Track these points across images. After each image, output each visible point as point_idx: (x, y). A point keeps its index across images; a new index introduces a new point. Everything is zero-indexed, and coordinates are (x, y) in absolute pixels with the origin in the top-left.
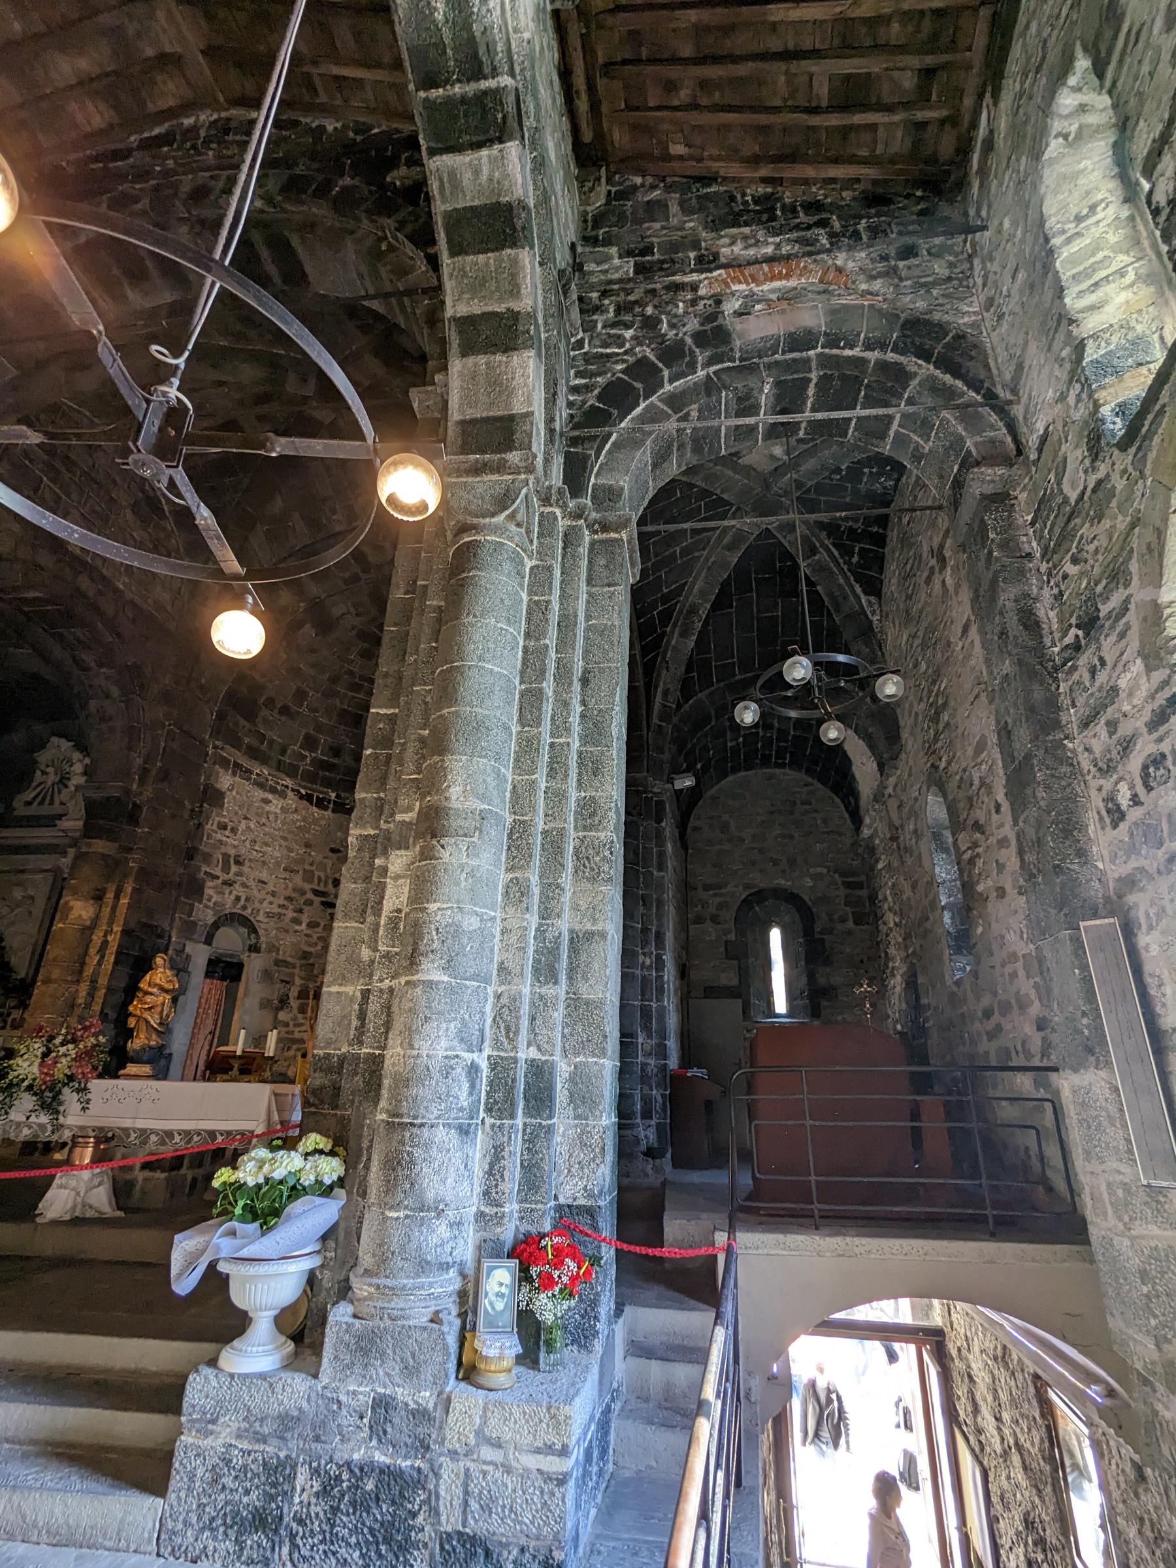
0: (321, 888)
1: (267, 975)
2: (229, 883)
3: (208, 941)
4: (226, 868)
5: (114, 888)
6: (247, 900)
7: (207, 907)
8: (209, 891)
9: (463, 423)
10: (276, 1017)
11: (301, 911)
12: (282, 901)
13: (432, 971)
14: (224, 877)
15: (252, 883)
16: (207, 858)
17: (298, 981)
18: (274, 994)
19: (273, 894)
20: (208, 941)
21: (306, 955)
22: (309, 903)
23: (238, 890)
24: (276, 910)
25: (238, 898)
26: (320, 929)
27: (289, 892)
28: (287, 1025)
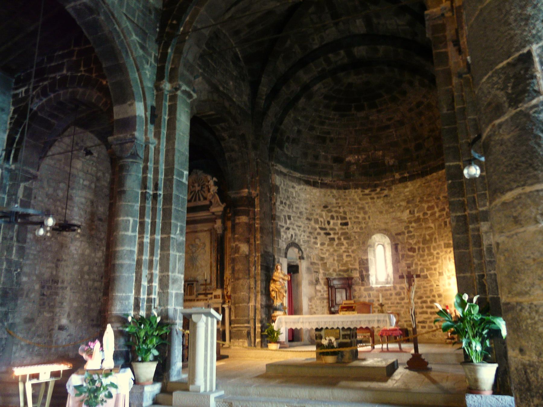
0: (323, 226)
1: (308, 269)
2: (288, 229)
3: (286, 257)
4: (286, 223)
5: (253, 237)
6: (296, 235)
7: (283, 241)
8: (282, 234)
10: (315, 288)
11: (316, 238)
12: (308, 234)
14: (286, 226)
15: (295, 227)
16: (279, 217)
17: (321, 271)
18: (313, 277)
19: (304, 231)
20: (286, 257)
21: (322, 259)
22: (319, 234)
23: (291, 232)
24: (306, 238)
25: (292, 235)
26: (326, 246)
27: (310, 230)
28: (320, 291)
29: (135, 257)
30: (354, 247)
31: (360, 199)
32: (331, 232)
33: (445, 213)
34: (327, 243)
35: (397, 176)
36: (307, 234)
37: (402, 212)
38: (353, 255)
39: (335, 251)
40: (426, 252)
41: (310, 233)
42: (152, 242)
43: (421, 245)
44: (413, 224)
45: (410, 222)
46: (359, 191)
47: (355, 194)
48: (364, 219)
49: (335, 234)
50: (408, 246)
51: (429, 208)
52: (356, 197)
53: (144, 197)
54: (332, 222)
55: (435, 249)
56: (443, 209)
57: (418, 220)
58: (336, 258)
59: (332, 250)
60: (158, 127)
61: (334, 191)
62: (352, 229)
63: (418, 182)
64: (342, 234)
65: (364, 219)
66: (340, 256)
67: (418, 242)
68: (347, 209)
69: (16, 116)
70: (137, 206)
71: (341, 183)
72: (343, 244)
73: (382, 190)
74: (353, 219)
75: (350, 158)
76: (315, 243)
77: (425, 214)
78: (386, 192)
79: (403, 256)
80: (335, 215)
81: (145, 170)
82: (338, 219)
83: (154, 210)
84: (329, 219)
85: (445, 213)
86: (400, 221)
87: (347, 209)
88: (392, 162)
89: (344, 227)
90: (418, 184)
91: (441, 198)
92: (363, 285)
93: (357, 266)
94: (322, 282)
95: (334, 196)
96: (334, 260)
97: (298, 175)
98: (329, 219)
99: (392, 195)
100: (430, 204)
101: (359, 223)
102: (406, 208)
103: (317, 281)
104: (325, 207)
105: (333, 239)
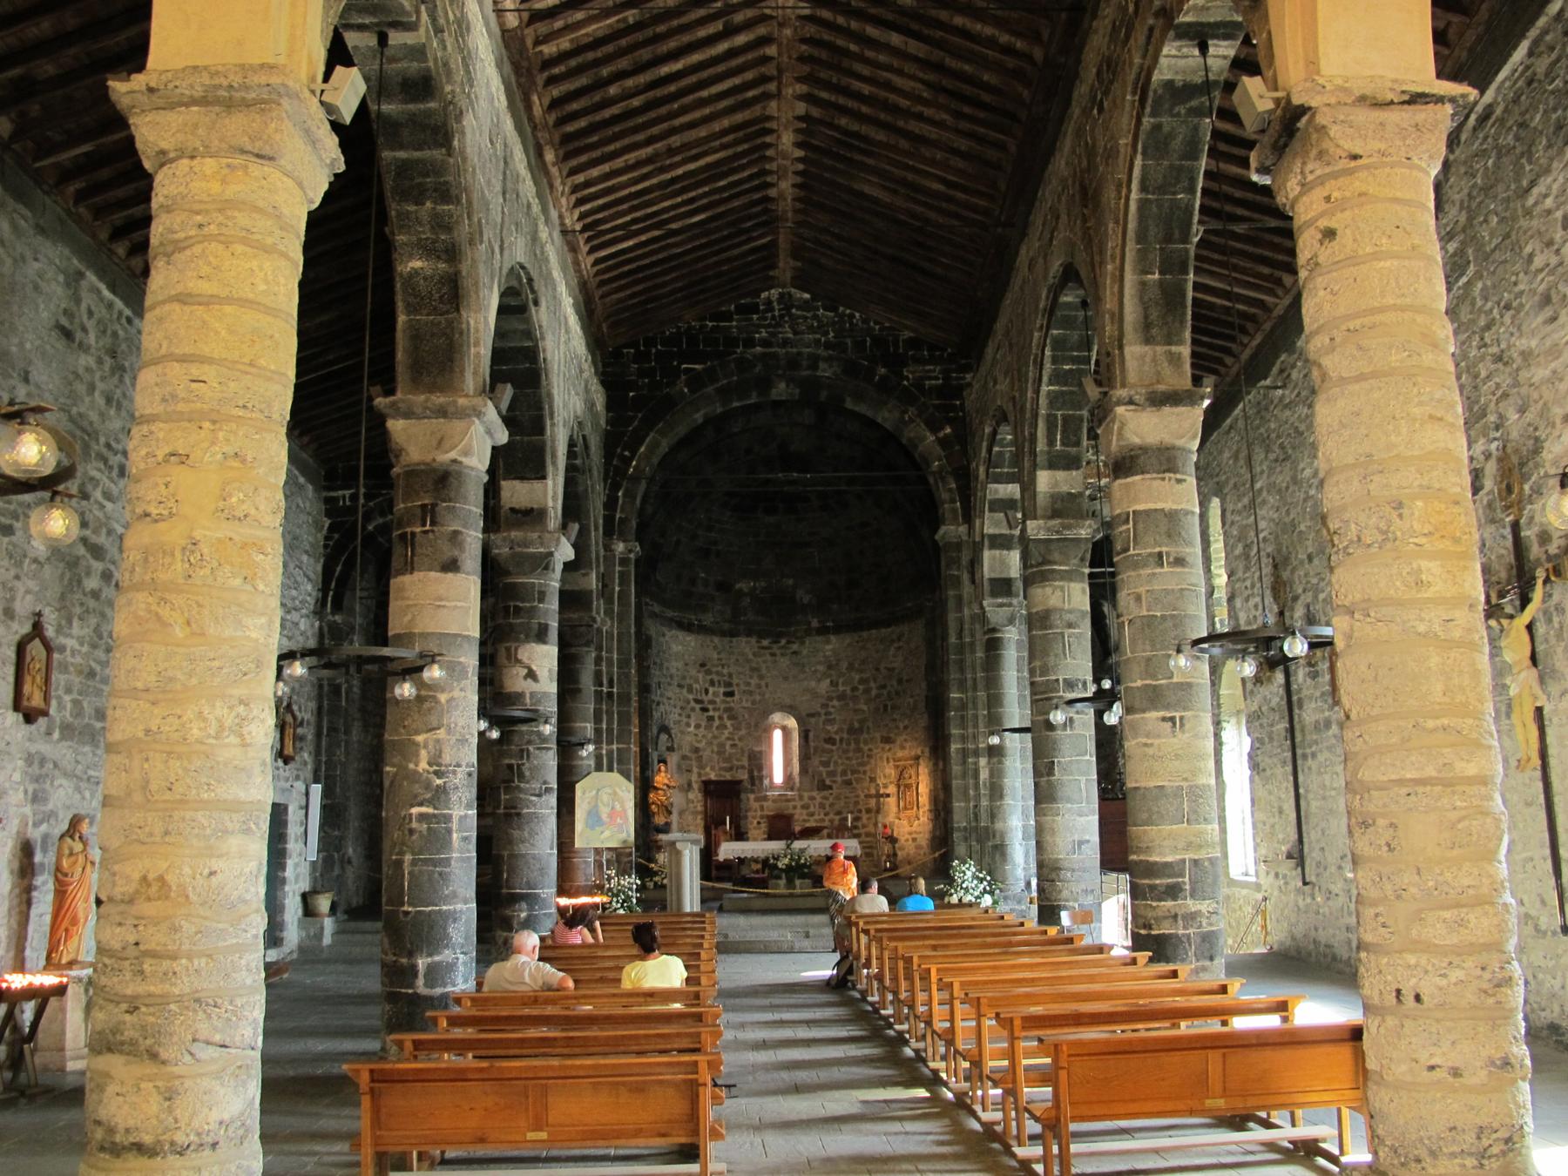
1: (679, 767)
9: (991, 580)
11: (689, 716)
13: (1008, 801)
17: (695, 770)
21: (697, 750)
22: (693, 709)
23: (662, 708)
30: (743, 732)
31: (754, 655)
33: (885, 692)
34: (703, 724)
35: (815, 623)
36: (678, 710)
37: (819, 680)
38: (740, 744)
39: (715, 737)
40: (853, 746)
42: (610, 753)
43: (845, 736)
44: (835, 703)
45: (830, 699)
46: (753, 640)
47: (746, 645)
48: (759, 686)
50: (823, 735)
51: (862, 681)
52: (747, 650)
53: (598, 694)
54: (711, 690)
55: (866, 743)
56: (884, 687)
57: (842, 697)
60: (610, 601)
61: (716, 640)
62: (740, 702)
63: (848, 639)
64: (728, 710)
65: (759, 686)
66: (722, 745)
67: (840, 730)
68: (733, 669)
69: (336, 536)
71: (726, 626)
72: (725, 727)
73: (789, 642)
74: (743, 687)
75: (743, 586)
76: (688, 725)
77: (854, 689)
78: (795, 647)
79: (816, 749)
80: (716, 678)
81: (598, 660)
83: (610, 713)
85: (885, 692)
86: (815, 695)
87: (733, 669)
88: (806, 599)
90: (848, 641)
91: (882, 666)
92: (753, 791)
93: (745, 762)
94: (695, 786)
95: (715, 648)
97: (670, 613)
99: (805, 652)
100: (865, 676)
101: (751, 693)
102: (825, 675)
103: (690, 785)
104: (703, 665)
105: (711, 719)
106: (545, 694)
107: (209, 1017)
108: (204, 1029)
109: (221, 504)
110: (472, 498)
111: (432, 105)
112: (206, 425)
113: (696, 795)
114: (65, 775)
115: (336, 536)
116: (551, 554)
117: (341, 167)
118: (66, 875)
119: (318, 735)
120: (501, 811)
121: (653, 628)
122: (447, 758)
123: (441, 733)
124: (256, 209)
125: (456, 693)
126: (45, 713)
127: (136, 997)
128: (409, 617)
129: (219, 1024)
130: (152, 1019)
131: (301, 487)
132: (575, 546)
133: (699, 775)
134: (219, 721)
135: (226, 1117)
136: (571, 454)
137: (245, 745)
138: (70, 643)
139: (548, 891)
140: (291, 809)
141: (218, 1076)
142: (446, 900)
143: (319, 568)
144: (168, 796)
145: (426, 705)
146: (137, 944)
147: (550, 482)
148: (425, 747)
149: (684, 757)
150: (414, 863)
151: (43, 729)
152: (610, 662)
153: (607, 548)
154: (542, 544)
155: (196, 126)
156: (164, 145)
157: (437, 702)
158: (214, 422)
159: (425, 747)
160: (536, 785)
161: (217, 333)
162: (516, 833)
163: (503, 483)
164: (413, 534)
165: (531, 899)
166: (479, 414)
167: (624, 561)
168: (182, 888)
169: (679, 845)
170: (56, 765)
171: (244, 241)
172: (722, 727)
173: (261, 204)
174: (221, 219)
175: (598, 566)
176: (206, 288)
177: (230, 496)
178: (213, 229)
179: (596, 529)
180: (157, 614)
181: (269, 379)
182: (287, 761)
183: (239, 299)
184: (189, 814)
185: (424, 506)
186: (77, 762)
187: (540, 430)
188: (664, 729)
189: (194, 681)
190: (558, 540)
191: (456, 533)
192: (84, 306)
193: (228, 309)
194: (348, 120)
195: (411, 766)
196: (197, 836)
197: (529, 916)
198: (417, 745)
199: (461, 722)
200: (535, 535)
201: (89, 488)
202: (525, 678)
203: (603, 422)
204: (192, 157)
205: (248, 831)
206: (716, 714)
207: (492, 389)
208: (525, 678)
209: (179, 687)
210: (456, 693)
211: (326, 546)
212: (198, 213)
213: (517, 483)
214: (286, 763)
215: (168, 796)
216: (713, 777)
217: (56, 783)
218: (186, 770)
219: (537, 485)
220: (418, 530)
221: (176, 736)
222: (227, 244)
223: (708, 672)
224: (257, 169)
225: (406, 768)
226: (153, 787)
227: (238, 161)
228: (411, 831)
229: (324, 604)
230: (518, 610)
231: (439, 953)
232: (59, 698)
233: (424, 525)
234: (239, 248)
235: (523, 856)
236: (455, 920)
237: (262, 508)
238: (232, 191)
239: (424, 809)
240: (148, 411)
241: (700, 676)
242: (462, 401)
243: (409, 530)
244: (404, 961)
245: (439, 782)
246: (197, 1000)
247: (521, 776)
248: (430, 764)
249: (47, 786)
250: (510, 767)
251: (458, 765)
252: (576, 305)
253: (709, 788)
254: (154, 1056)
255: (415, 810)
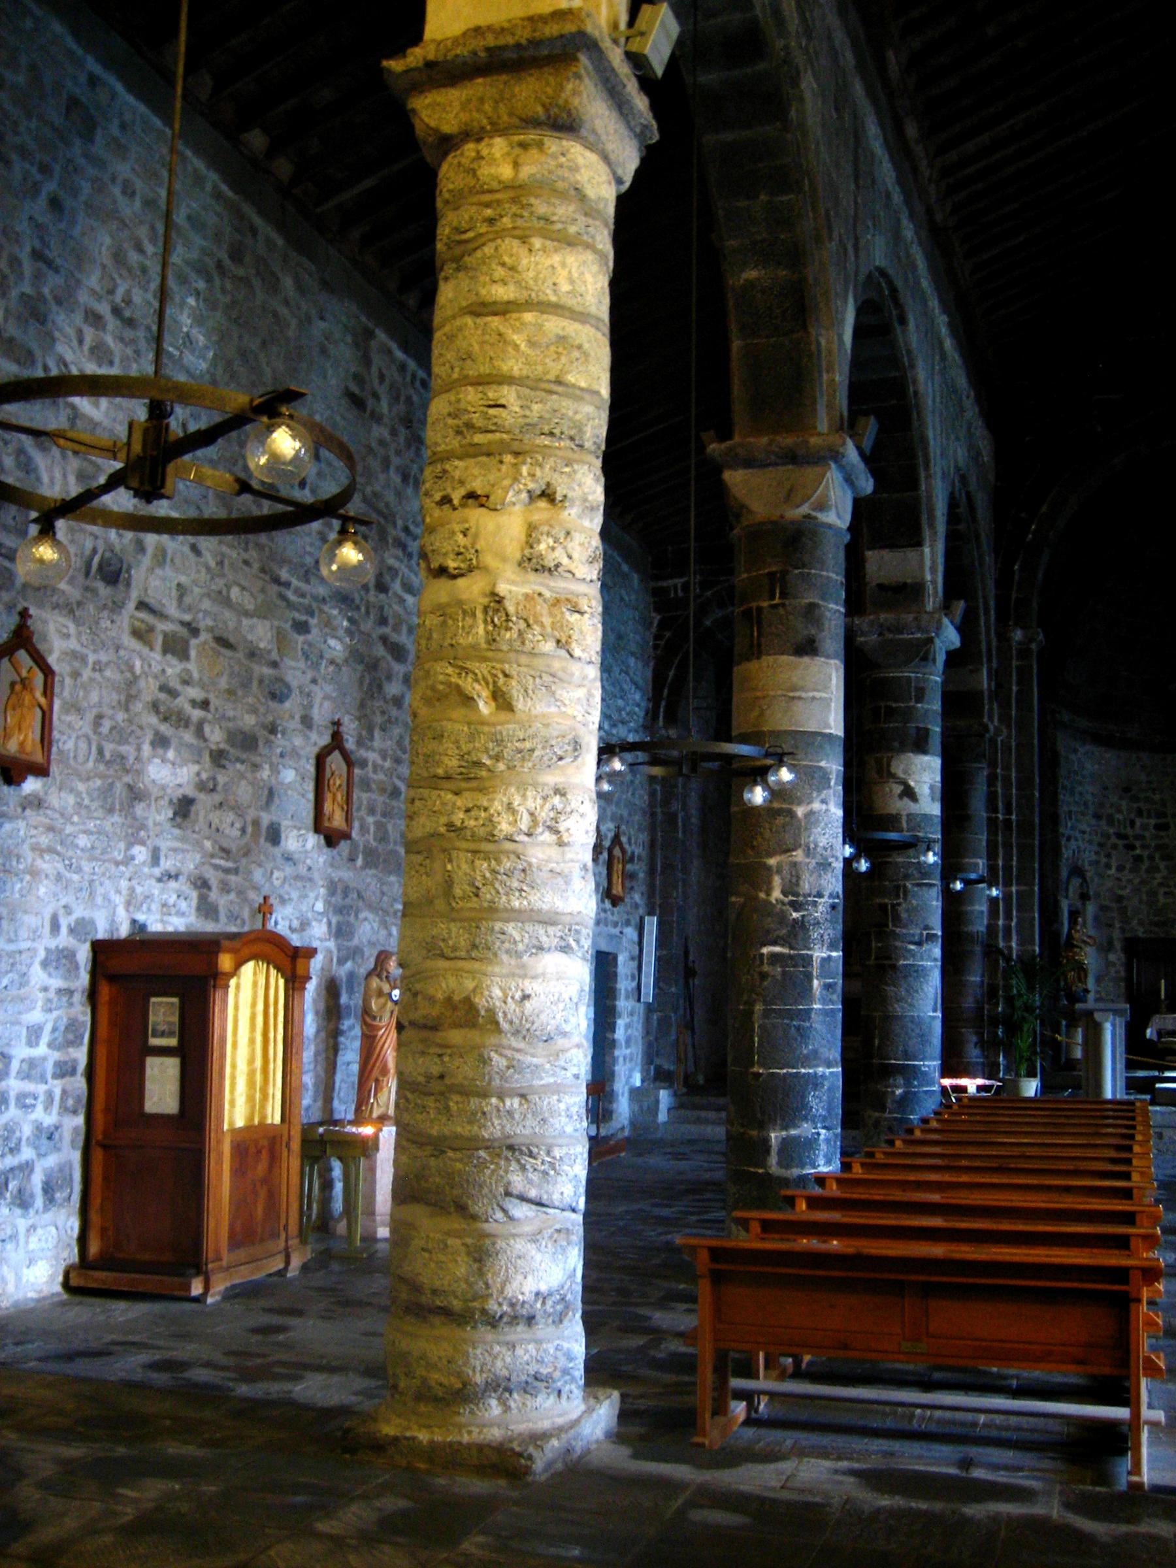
1: (1096, 918)
2: (1069, 839)
11: (1108, 856)
17: (1117, 925)
19: (1090, 842)
21: (1120, 899)
22: (1115, 847)
24: (1094, 857)
26: (1126, 872)
29: (985, 922)
32: (1138, 844)
34: (1128, 866)
36: (1096, 848)
39: (1142, 882)
41: (1101, 845)
49: (1143, 847)
53: (992, 823)
58: (1144, 897)
59: (1137, 881)
64: (1158, 848)
66: (1153, 894)
69: (668, 634)
70: (984, 837)
72: (1157, 870)
76: (1108, 866)
81: (992, 780)
82: (1149, 817)
83: (1007, 846)
84: (1132, 816)
89: (1162, 834)
94: (1118, 945)
96: (1141, 902)
98: (1132, 816)
104: (1127, 790)
106: (927, 817)
107: (523, 1168)
108: (517, 1181)
109: (527, 552)
110: (831, 563)
111: (761, 66)
112: (508, 458)
113: (1116, 957)
114: (370, 907)
115: (668, 634)
116: (930, 641)
117: (656, 137)
118: (374, 1018)
119: (652, 871)
120: (872, 962)
121: (1063, 742)
122: (806, 886)
123: (799, 855)
124: (556, 192)
125: (816, 806)
126: (347, 836)
127: (442, 1138)
128: (756, 713)
129: (534, 1177)
130: (459, 1165)
131: (625, 576)
132: (959, 629)
133: (1123, 930)
134: (532, 814)
135: (543, 1288)
136: (953, 517)
137: (561, 844)
138: (372, 756)
139: (932, 1064)
140: (621, 959)
141: (534, 1238)
142: (806, 1061)
143: (649, 673)
144: (474, 903)
145: (780, 820)
146: (442, 1077)
147: (927, 550)
148: (779, 872)
149: (1103, 908)
150: (766, 1014)
151: (345, 853)
152: (1007, 780)
153: (1003, 637)
154: (919, 629)
155: (482, 100)
156: (447, 129)
157: (791, 814)
158: (517, 454)
159: (779, 872)
160: (915, 931)
161: (516, 347)
162: (891, 990)
163: (869, 554)
164: (759, 609)
165: (910, 1074)
166: (836, 456)
167: (1024, 653)
168: (491, 1012)
169: (1098, 1016)
170: (360, 896)
171: (546, 235)
172: (1153, 869)
173: (560, 185)
174: (514, 209)
175: (989, 661)
176: (502, 293)
177: (539, 542)
178: (506, 221)
179: (987, 612)
180: (458, 687)
181: (579, 399)
182: (615, 901)
183: (540, 303)
184: (498, 926)
185: (771, 575)
186: (383, 893)
187: (914, 484)
188: (1077, 871)
189: (501, 766)
190: (939, 623)
191: (812, 607)
192: (374, 369)
193: (528, 317)
194: (659, 71)
195: (762, 895)
196: (508, 952)
197: (906, 1094)
198: (769, 868)
199: (823, 842)
200: (911, 617)
201: (387, 578)
202: (901, 796)
203: (991, 477)
204: (479, 140)
205: (565, 949)
206: (1146, 853)
207: (852, 424)
208: (901, 796)
209: (484, 773)
210: (816, 806)
211: (656, 647)
212: (487, 205)
213: (886, 554)
214: (614, 904)
215: (474, 903)
216: (1140, 933)
217: (362, 915)
218: (494, 872)
219: (911, 554)
220: (765, 604)
221: (482, 832)
222: (524, 239)
223: (1135, 799)
224: (553, 145)
225: (756, 898)
226: (458, 892)
227: (531, 136)
228: (763, 976)
229: (655, 717)
230: (891, 712)
231: (795, 1126)
232: (362, 820)
233: (772, 597)
234: (537, 242)
235: (897, 1018)
236: (816, 1086)
237: (575, 556)
238: (527, 171)
239: (777, 949)
240: (442, 447)
241: (1124, 803)
242: (813, 440)
243: (754, 605)
244: (754, 1133)
245: (795, 915)
246: (511, 1148)
247: (897, 919)
248: (784, 893)
249: (352, 919)
250: (883, 907)
251: (820, 895)
252: (951, 325)
253: (1132, 947)
254: (461, 1209)
255: (765, 950)
